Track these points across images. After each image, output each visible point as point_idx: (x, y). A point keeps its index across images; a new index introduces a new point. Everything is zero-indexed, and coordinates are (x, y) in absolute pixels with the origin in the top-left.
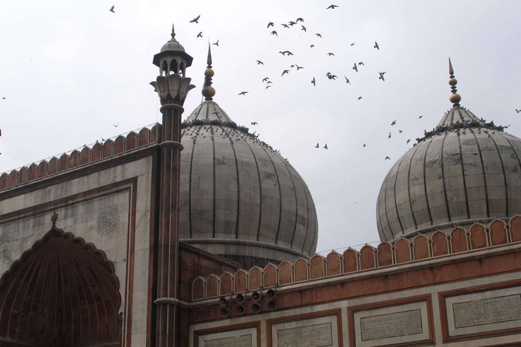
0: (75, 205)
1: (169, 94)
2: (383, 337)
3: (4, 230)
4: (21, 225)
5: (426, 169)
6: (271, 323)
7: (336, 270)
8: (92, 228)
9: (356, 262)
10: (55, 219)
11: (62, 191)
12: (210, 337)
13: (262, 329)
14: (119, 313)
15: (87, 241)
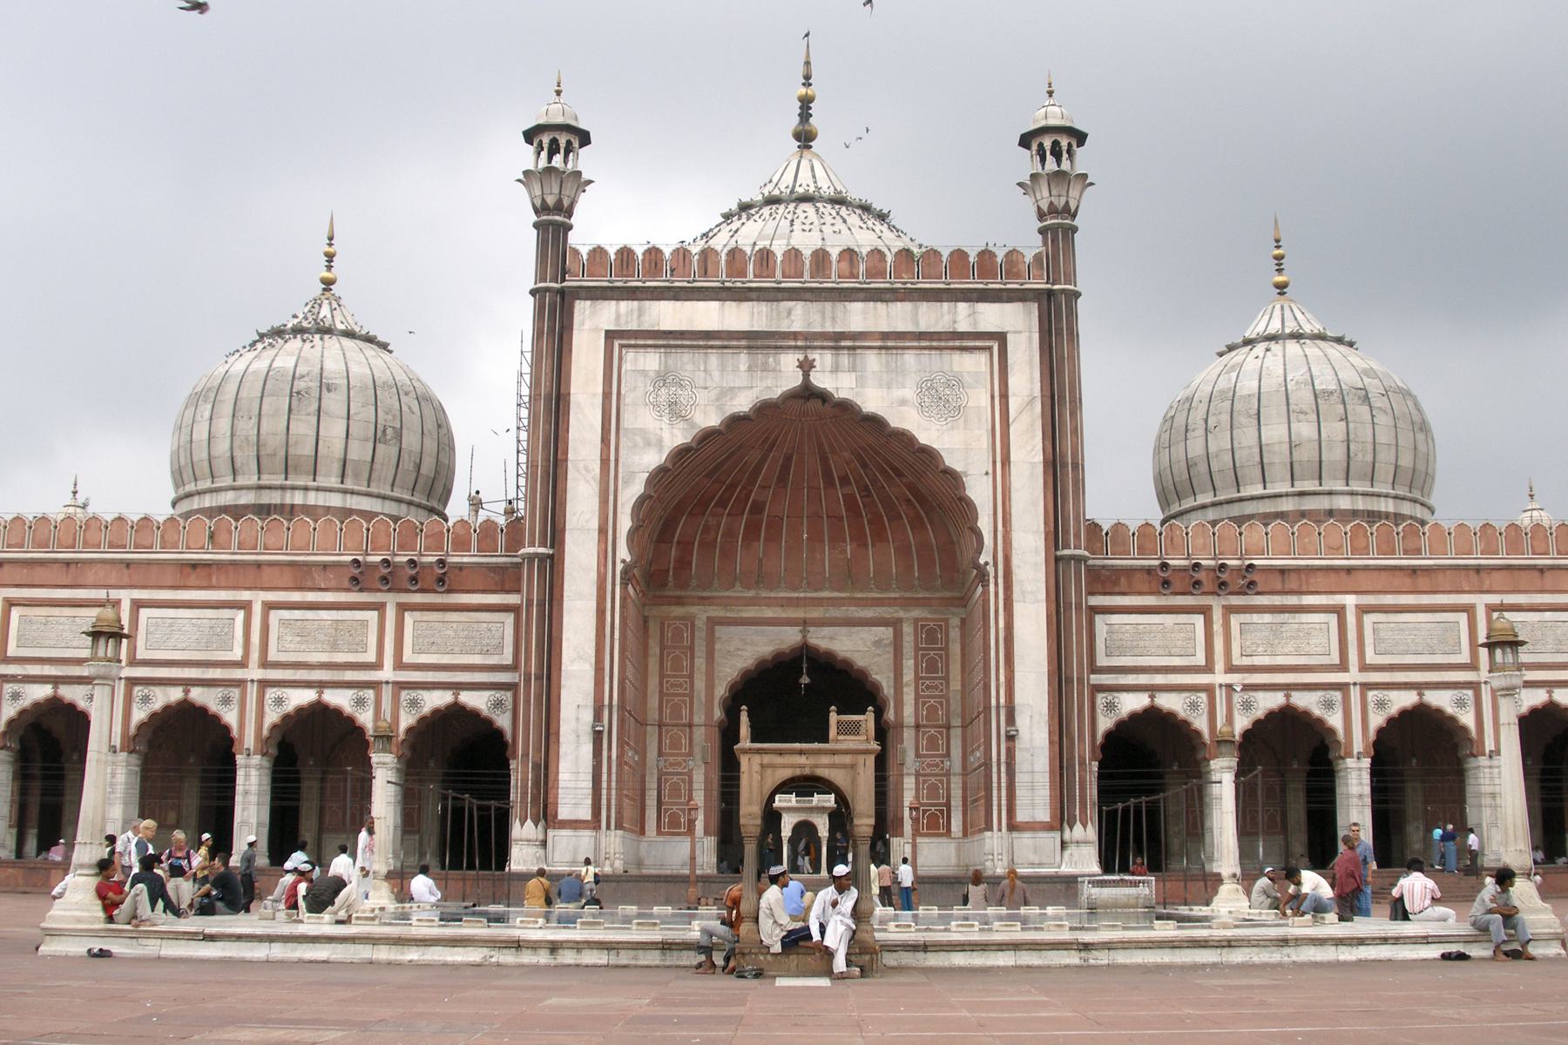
0: (858, 351)
1: (1067, 202)
2: (1407, 653)
3: (666, 362)
4: (714, 359)
5: (1319, 400)
6: (1229, 610)
7: (1338, 549)
8: (903, 402)
9: (1368, 542)
10: (806, 367)
11: (824, 318)
12: (1116, 619)
13: (1215, 618)
14: (982, 561)
15: (895, 422)
